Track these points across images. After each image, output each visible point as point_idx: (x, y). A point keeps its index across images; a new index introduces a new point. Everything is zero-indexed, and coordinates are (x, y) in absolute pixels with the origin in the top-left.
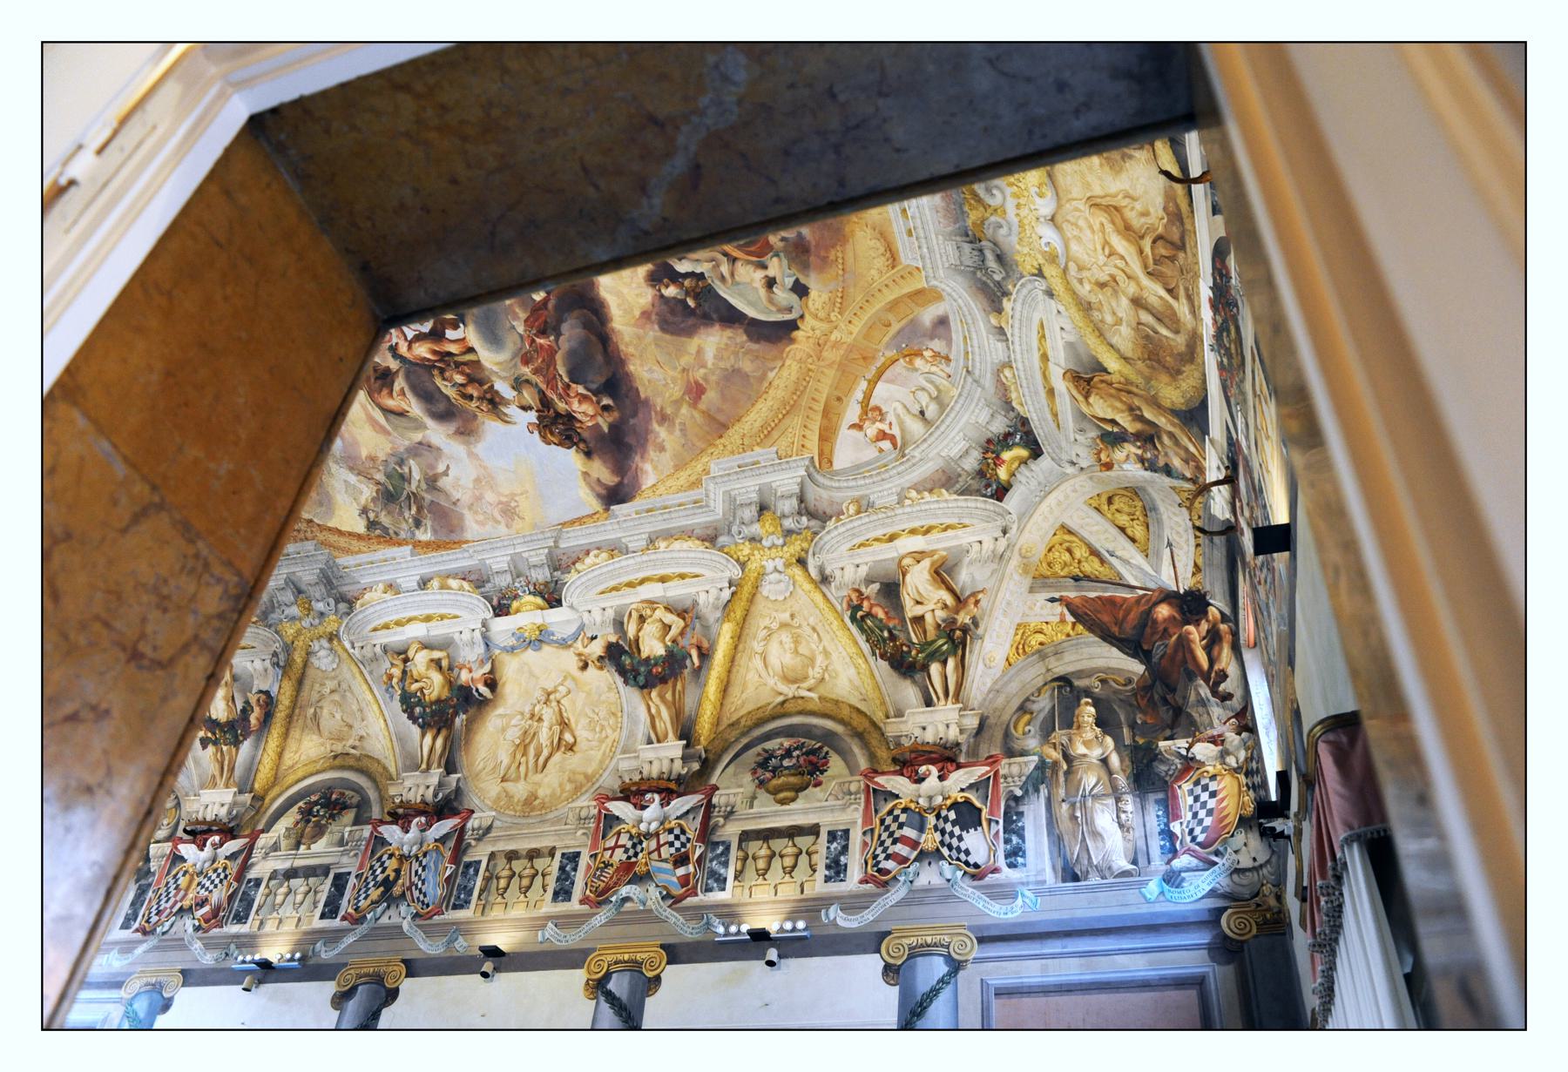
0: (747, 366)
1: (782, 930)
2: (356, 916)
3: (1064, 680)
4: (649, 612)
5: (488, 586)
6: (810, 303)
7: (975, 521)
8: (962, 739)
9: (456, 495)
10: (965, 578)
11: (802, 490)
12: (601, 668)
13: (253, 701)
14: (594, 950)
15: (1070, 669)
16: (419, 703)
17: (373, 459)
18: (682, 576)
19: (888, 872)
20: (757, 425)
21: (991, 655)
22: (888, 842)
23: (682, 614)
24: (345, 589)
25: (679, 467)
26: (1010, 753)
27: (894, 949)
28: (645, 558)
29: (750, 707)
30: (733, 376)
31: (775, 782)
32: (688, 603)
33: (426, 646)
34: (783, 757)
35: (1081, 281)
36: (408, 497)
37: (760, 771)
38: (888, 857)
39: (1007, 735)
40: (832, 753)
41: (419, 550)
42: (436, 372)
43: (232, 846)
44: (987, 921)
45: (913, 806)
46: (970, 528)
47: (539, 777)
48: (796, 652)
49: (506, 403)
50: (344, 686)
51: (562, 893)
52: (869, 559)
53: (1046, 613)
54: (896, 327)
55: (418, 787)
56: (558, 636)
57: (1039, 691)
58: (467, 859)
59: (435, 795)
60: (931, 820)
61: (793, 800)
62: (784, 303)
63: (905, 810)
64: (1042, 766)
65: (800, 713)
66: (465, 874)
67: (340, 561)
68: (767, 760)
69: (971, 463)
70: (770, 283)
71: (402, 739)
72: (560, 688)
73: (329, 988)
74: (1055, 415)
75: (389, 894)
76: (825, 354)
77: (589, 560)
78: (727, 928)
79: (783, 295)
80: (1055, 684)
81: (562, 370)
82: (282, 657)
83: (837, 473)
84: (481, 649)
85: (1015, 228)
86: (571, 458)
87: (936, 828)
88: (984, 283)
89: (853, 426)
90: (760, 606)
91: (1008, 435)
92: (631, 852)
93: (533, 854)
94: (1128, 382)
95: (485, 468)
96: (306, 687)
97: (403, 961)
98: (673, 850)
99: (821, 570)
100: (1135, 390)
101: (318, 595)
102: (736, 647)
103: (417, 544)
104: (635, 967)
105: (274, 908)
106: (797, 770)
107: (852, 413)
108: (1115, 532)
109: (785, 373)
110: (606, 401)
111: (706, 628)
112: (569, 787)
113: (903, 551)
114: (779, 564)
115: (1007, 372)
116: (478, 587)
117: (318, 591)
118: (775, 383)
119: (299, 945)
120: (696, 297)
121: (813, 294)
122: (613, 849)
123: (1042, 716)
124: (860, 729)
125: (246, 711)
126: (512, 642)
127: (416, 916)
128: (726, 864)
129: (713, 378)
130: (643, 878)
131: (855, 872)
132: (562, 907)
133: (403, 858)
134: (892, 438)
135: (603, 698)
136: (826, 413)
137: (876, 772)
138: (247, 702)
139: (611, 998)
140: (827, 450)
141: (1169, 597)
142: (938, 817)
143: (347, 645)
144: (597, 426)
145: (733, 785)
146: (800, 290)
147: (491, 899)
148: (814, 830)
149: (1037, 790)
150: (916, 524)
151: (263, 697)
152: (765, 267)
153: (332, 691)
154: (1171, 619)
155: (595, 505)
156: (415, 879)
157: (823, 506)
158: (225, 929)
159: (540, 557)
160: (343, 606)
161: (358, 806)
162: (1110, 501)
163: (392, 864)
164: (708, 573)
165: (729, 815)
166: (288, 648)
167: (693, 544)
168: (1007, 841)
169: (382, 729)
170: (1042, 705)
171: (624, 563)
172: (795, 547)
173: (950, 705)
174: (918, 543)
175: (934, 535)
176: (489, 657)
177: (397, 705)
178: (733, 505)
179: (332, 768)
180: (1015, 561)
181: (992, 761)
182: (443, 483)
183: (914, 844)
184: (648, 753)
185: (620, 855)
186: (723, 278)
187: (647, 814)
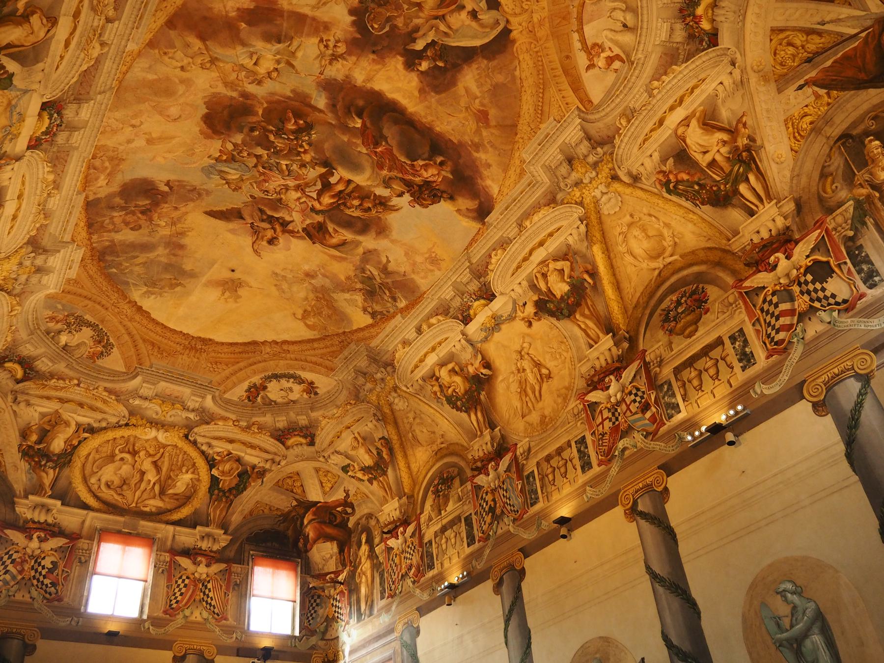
0: (500, 78)
1: (728, 417)
2: (485, 536)
3: (845, 136)
4: (546, 269)
5: (451, 310)
6: (506, 8)
7: (707, 72)
8: (788, 223)
9: (402, 270)
10: (725, 114)
11: (585, 133)
12: (539, 320)
13: (380, 446)
14: (619, 491)
15: (844, 126)
16: (458, 399)
17: (348, 278)
18: (551, 235)
19: (783, 341)
20: (532, 111)
21: (778, 154)
22: (773, 321)
23: (565, 257)
24: (384, 358)
25: (506, 170)
26: (830, 211)
27: (815, 390)
28: (523, 238)
29: (640, 289)
30: (496, 91)
31: (679, 326)
32: (564, 249)
33: (442, 365)
34: (676, 308)
36: (380, 288)
37: (666, 325)
38: (777, 332)
39: (821, 200)
40: (706, 286)
42: (342, 207)
43: (410, 529)
44: (873, 335)
45: (778, 288)
46: (708, 79)
47: (540, 405)
48: (648, 237)
49: (389, 199)
50: (418, 412)
51: (586, 466)
52: (655, 146)
53: (800, 100)
55: (482, 446)
56: (505, 315)
57: (829, 156)
58: (526, 474)
59: (493, 446)
60: (796, 289)
61: (696, 330)
62: (491, 21)
63: (773, 294)
64: (858, 205)
65: (673, 274)
66: (528, 483)
68: (667, 315)
69: (680, 35)
70: (474, 14)
71: (460, 425)
72: (525, 345)
73: (489, 585)
75: (496, 516)
76: (538, 35)
77: (493, 261)
78: (692, 435)
79: (487, 17)
80: (839, 143)
81: (403, 159)
82: (378, 414)
83: (599, 105)
84: (470, 349)
86: (444, 207)
87: (802, 293)
89: (588, 68)
90: (608, 222)
92: (614, 419)
93: (559, 451)
96: (401, 424)
97: (519, 550)
98: (637, 404)
99: (630, 174)
102: (609, 258)
103: (402, 311)
104: (649, 489)
105: (444, 552)
106: (689, 310)
107: (582, 60)
109: (524, 65)
110: (439, 159)
111: (584, 257)
112: (560, 400)
113: (673, 126)
114: (602, 188)
116: (447, 315)
117: (373, 369)
118: (523, 77)
119: (464, 567)
120: (441, 58)
122: (602, 423)
123: (840, 172)
124: (717, 259)
125: (379, 453)
126: (483, 334)
127: (514, 520)
128: (673, 395)
129: (486, 101)
130: (627, 432)
131: (760, 354)
132: (590, 474)
133: (493, 491)
134: (618, 57)
135: (551, 336)
136: (566, 72)
137: (741, 280)
138: (377, 448)
139: (643, 515)
142: (800, 284)
143: (404, 389)
145: (654, 344)
147: (549, 490)
148: (719, 342)
149: (864, 224)
150: (671, 102)
151: (383, 441)
152: (463, 7)
153: (414, 419)
155: (475, 226)
156: (504, 500)
158: (427, 576)
159: (466, 276)
160: (389, 368)
161: (459, 474)
163: (489, 498)
164: (564, 223)
165: (661, 363)
166: (379, 408)
167: (544, 211)
168: (859, 272)
169: (448, 423)
170: (836, 164)
171: (513, 249)
172: (605, 171)
173: (767, 206)
174: (680, 114)
175: (687, 101)
176: (477, 351)
177: (447, 407)
178: (551, 171)
179: (437, 461)
180: (753, 79)
181: (819, 224)
182: (392, 267)
183: (791, 312)
184: (593, 354)
185: (608, 425)
186: (446, 34)
187: (611, 391)
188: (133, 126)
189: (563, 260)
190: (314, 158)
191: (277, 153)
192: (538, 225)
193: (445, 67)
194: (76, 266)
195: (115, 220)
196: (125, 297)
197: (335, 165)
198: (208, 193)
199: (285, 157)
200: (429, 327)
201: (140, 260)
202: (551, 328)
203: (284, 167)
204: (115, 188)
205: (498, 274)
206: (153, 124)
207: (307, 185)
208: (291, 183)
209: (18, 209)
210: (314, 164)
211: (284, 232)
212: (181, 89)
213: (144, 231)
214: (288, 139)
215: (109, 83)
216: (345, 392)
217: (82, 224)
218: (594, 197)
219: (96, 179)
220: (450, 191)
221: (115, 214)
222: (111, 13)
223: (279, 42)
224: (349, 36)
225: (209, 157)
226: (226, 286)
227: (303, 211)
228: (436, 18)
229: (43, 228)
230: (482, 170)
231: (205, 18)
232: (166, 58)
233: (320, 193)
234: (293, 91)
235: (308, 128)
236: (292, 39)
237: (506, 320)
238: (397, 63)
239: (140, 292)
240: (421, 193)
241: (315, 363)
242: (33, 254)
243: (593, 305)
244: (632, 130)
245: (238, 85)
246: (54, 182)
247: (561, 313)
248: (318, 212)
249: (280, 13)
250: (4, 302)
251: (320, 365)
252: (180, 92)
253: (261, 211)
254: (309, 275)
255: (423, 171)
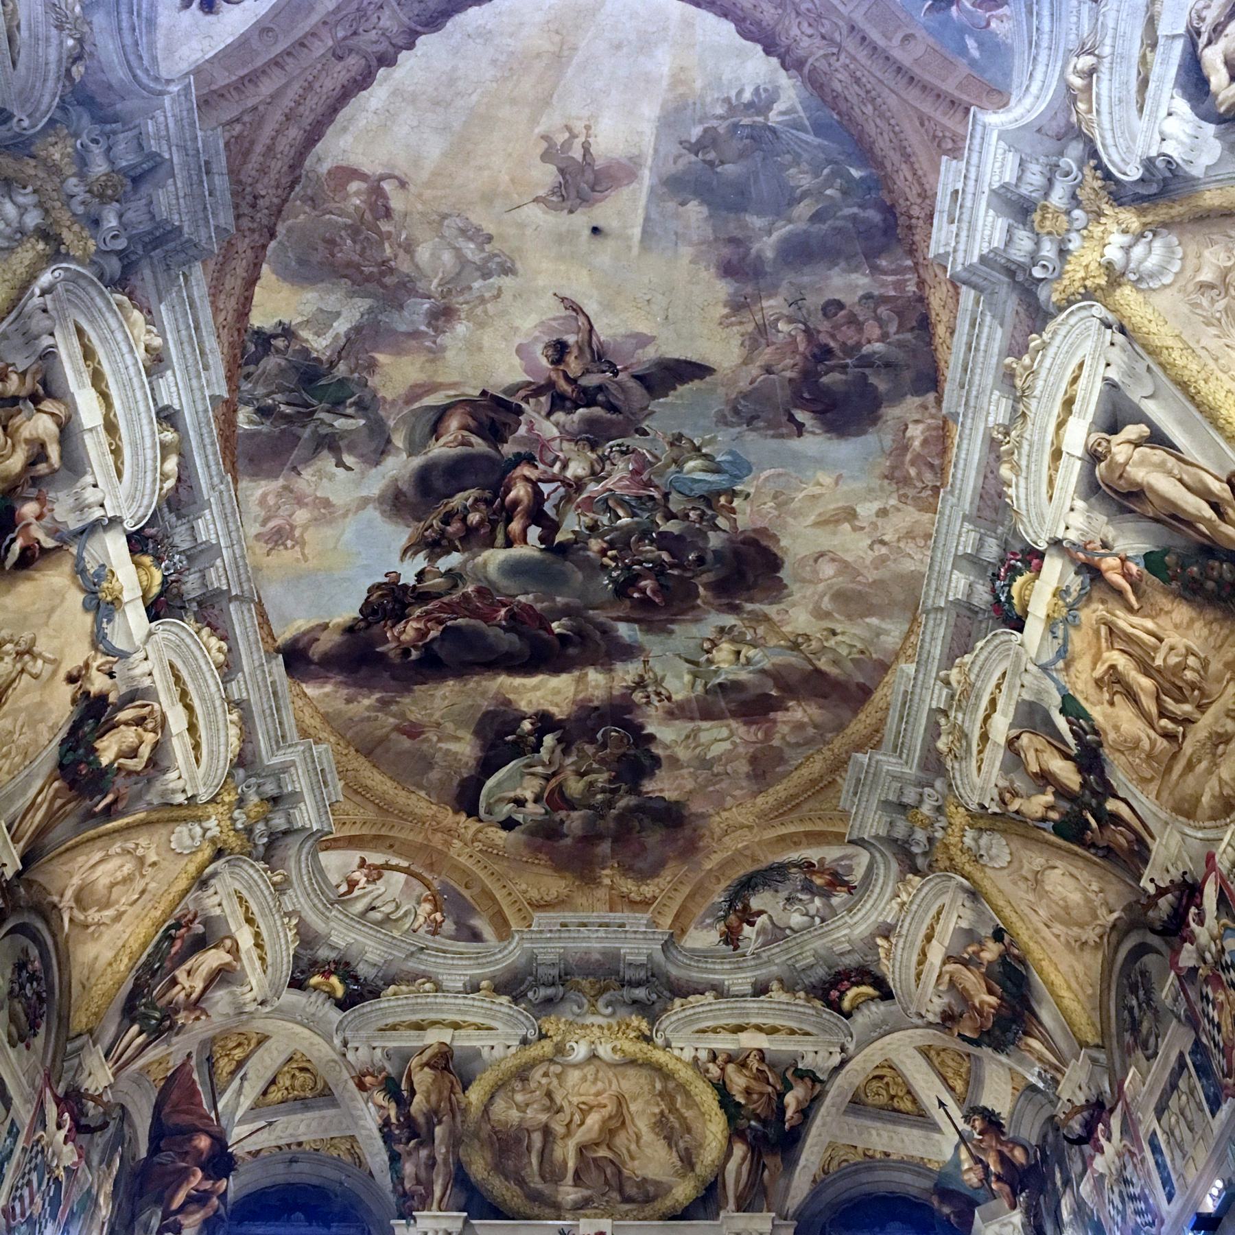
0: (435, 775)
4: (150, 726)
9: (307, 473)
12: (74, 701)
18: (197, 747)
20: (369, 782)
23: (152, 762)
25: (326, 718)
28: (218, 703)
30: (428, 763)
32: (165, 764)
35: (546, 1075)
36: (307, 405)
41: (222, 409)
42: (487, 494)
48: (113, 885)
49: (432, 558)
54: (466, 894)
61: (13, 1046)
62: (497, 809)
67: (198, 271)
69: (323, 953)
70: (520, 802)
72: (40, 662)
74: (394, 1028)
77: (214, 642)
79: (506, 809)
84: (74, 524)
85: (580, 1020)
88: (522, 982)
89: (363, 861)
90: (163, 831)
91: (356, 979)
94: (465, 1111)
95: (345, 515)
99: (214, 875)
100: (459, 1119)
101: (130, 215)
107: (375, 858)
108: (269, 1075)
109: (423, 804)
110: (415, 654)
111: (139, 796)
113: (238, 936)
114: (215, 831)
115: (428, 986)
116: (168, 502)
120: (514, 742)
121: (504, 834)
126: (92, 567)
129: (425, 746)
134: (350, 891)
140: (341, 844)
141: (219, 1141)
143: (46, 279)
144: (386, 641)
146: (509, 824)
152: (536, 801)
154: (200, 1152)
157: (279, 853)
159: (216, 580)
160: (114, 266)
162: (302, 1069)
167: (235, 742)
171: (211, 681)
175: (255, 953)
182: (327, 462)
188: (883, 543)
189: (150, 759)
190: (586, 548)
191: (645, 534)
192: (222, 733)
193: (502, 738)
194: (943, 202)
195: (877, 332)
196: (816, 83)
197: (548, 556)
198: (722, 421)
199: (627, 532)
200: (164, 446)
201: (804, 209)
202: (52, 728)
203: (621, 513)
204: (891, 413)
205: (188, 641)
206: (853, 545)
207: (567, 499)
208: (593, 488)
209: (1061, 425)
210: (579, 541)
211: (550, 385)
212: (826, 604)
213: (814, 301)
214: (640, 563)
215: (931, 623)
216: (119, 74)
217: (941, 330)
218: (209, 818)
219: (925, 442)
220: (362, 634)
221: (878, 346)
222: (943, 721)
223: (720, 685)
224: (638, 712)
225: (748, 495)
226: (589, 176)
227: (544, 446)
228: (554, 774)
229: (1018, 349)
230: (352, 691)
231: (825, 697)
232: (859, 645)
233: (538, 497)
234: (671, 632)
235: (622, 590)
236: (707, 692)
237: (100, 628)
238: (559, 713)
239: (779, 107)
240: (396, 600)
241: (252, 79)
242: (1037, 273)
243: (66, 815)
244: (263, 886)
245: (750, 620)
246: (998, 458)
247: (70, 749)
248: (519, 459)
249: (734, 715)
250: (1105, 118)
251: (240, 85)
252: (826, 599)
253: (612, 408)
254: (443, 315)
255: (421, 625)
